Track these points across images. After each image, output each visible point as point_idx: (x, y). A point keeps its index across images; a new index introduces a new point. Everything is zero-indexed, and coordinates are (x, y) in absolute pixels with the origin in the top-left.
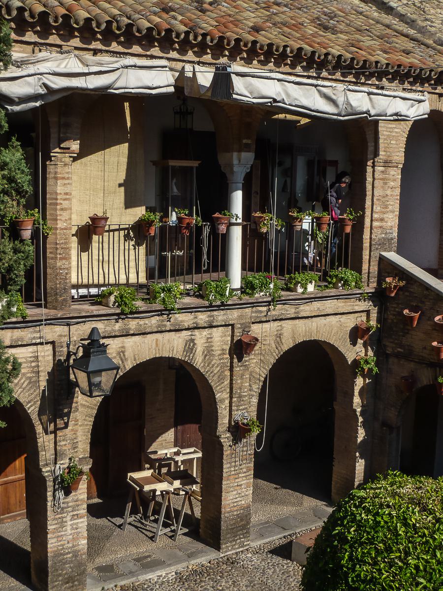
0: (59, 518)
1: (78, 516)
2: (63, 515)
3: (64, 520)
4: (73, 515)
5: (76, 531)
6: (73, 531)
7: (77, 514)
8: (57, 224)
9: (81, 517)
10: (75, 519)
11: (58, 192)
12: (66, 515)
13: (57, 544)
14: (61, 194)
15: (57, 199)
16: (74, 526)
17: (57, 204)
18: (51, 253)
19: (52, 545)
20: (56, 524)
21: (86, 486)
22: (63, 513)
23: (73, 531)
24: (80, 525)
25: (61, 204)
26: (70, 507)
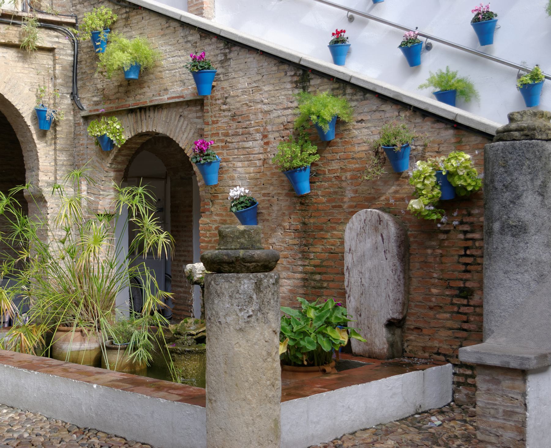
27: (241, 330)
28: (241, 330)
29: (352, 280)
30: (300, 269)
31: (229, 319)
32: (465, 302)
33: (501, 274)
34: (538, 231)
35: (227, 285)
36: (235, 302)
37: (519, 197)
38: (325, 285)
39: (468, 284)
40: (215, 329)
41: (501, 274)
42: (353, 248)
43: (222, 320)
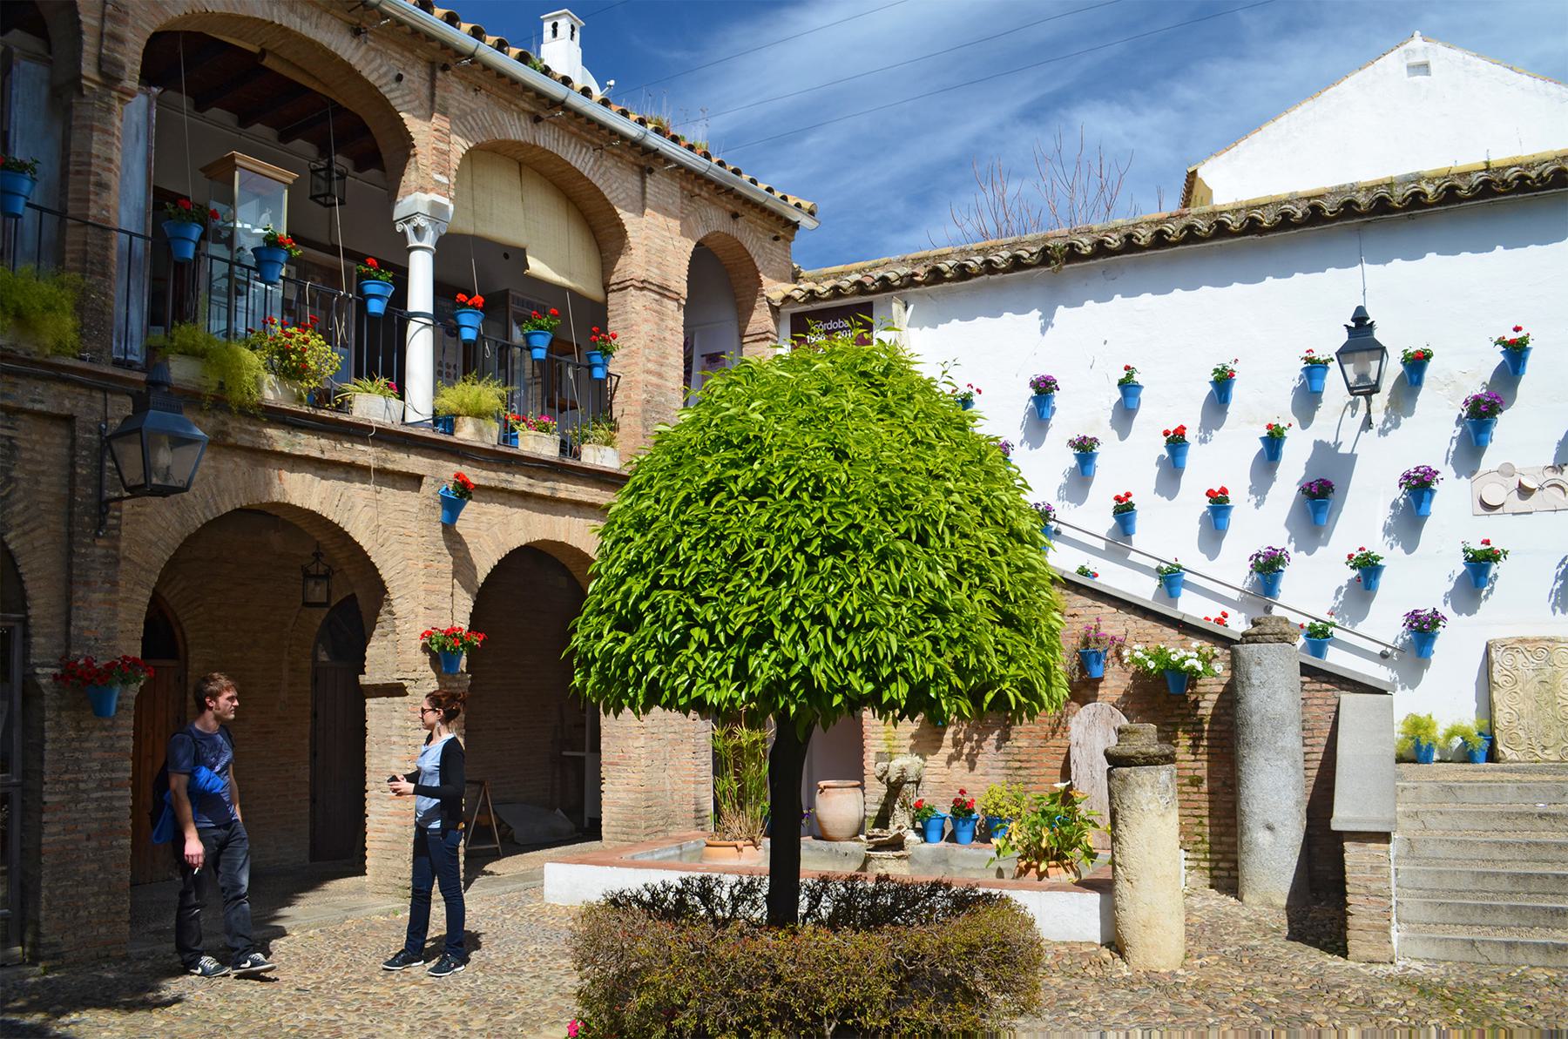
0: (70, 781)
1: (114, 785)
2: (79, 776)
3: (82, 786)
4: (102, 780)
5: (107, 814)
6: (100, 815)
7: (110, 779)
8: (88, 209)
9: (120, 787)
10: (106, 789)
11: (94, 152)
12: (85, 777)
13: (62, 837)
14: (98, 157)
15: (90, 164)
16: (104, 805)
17: (89, 172)
18: (72, 260)
19: (51, 839)
20: (63, 793)
21: (131, 722)
22: (79, 771)
23: (100, 815)
24: (117, 804)
25: (99, 175)
26: (95, 760)
27: (1162, 815)
28: (1162, 815)
29: (1081, 773)
30: (1002, 764)
31: (1151, 806)
32: (1195, 789)
33: (1262, 761)
34: (1292, 722)
35: (1148, 776)
36: (1156, 791)
37: (1275, 693)
38: (1034, 779)
39: (1198, 773)
40: (1136, 815)
41: (1262, 761)
42: (1081, 742)
43: (1145, 808)
